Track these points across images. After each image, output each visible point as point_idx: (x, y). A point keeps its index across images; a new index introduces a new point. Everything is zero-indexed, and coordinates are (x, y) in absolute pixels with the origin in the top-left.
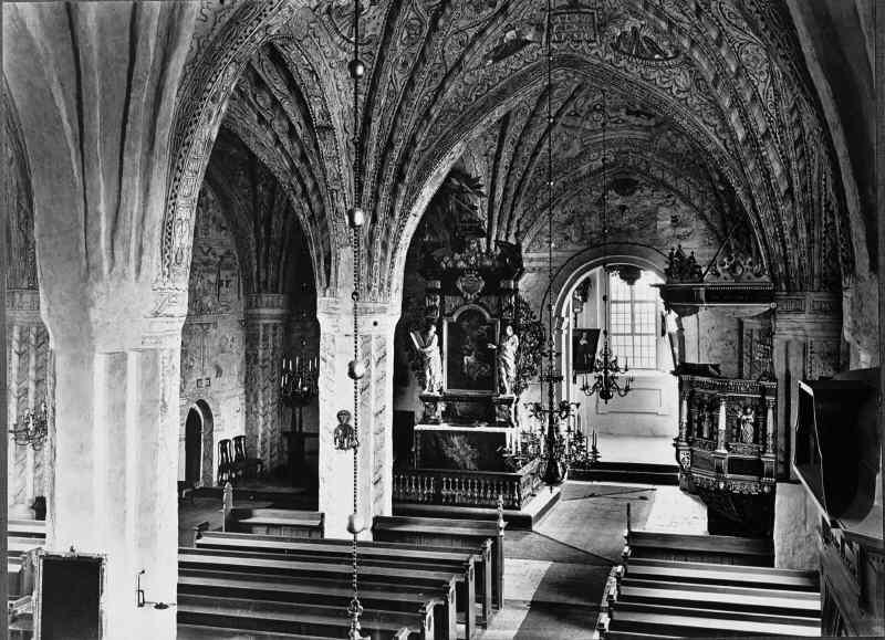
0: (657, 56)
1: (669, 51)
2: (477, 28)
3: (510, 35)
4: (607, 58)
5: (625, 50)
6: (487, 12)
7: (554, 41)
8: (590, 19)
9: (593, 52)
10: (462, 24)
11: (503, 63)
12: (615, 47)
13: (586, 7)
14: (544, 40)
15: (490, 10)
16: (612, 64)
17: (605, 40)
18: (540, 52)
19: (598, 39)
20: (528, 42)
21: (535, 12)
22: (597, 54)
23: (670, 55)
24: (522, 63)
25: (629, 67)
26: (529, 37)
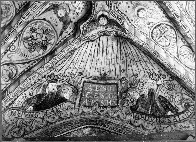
0: (169, 113)
1: (179, 106)
2: (27, 65)
3: (52, 87)
4: (127, 119)
5: (143, 111)
6: (38, 53)
7: (85, 106)
8: (113, 88)
9: (116, 115)
10: (16, 57)
11: (41, 114)
12: (134, 109)
13: (111, 79)
14: (78, 102)
15: (41, 52)
16: (131, 124)
17: (126, 104)
18: (73, 112)
19: (120, 105)
20: (64, 100)
21: (74, 72)
22: (118, 116)
23: (181, 110)
24: (57, 117)
25: (145, 125)
26: (67, 96)
